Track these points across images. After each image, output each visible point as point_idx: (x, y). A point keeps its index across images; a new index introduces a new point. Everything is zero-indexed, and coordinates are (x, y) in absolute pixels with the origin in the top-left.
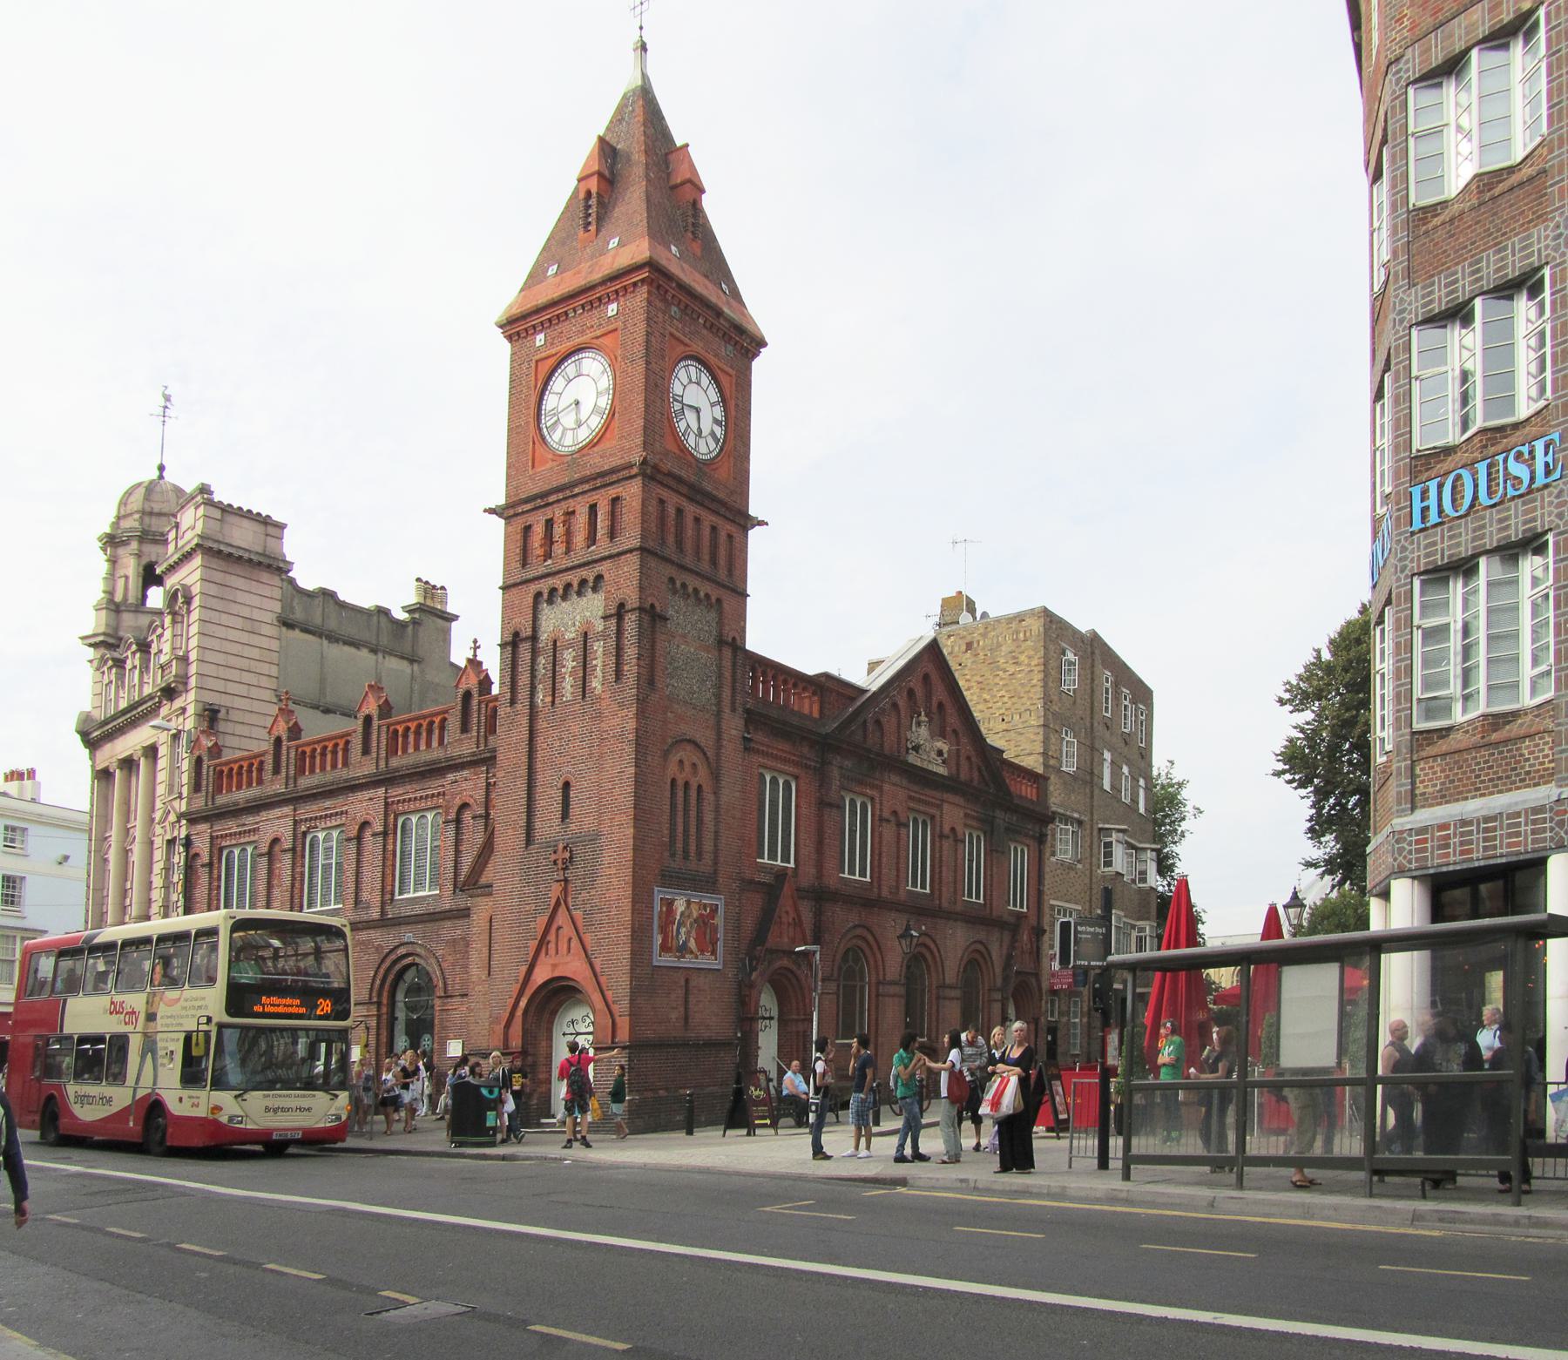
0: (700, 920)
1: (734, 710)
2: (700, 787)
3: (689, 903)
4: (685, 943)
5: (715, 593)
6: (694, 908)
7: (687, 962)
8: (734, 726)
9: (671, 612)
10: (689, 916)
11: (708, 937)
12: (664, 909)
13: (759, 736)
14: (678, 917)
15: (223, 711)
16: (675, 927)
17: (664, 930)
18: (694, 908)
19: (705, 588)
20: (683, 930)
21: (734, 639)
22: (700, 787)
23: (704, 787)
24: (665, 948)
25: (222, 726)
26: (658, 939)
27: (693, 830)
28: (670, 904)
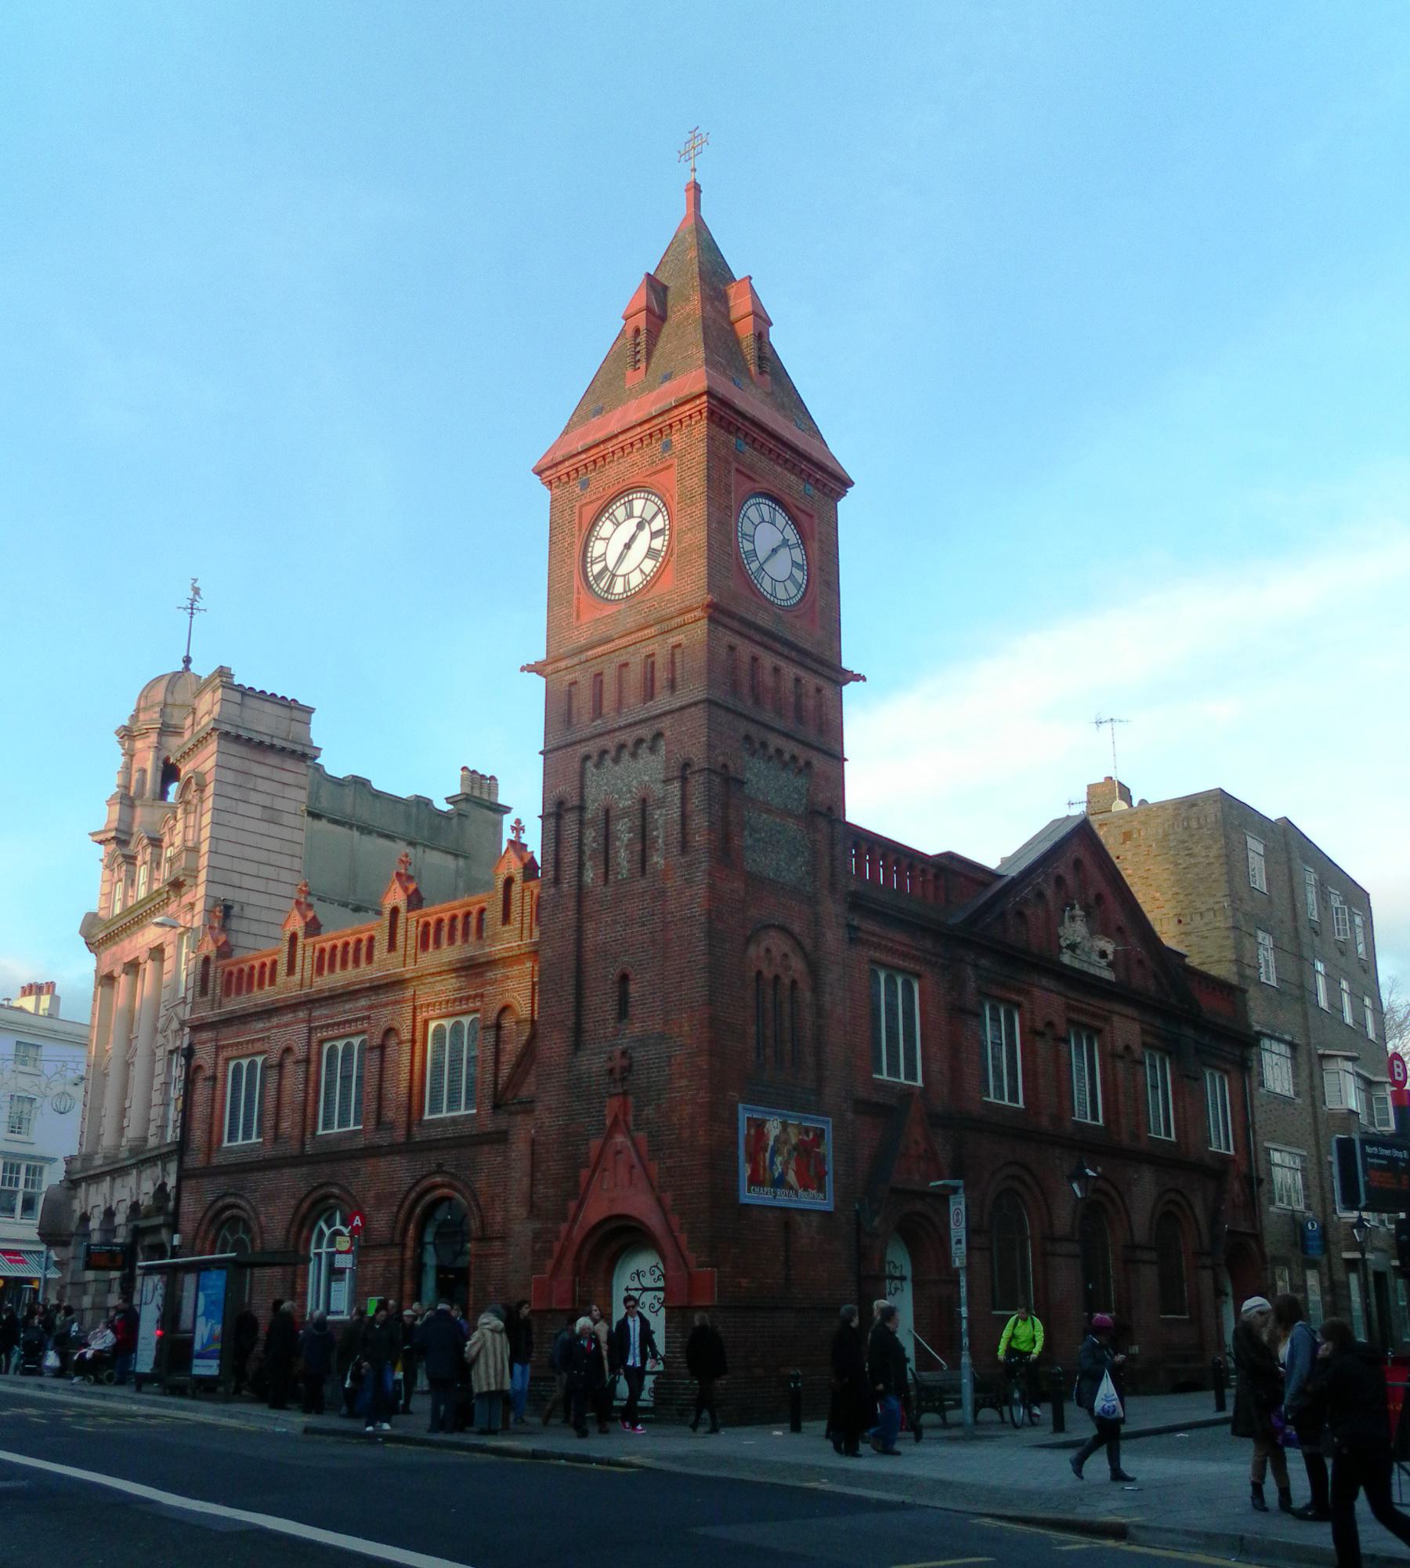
2: (794, 982)
3: (785, 1125)
4: (783, 1175)
5: (803, 754)
6: (792, 1132)
7: (784, 1199)
12: (753, 1132)
14: (771, 1143)
16: (768, 1155)
17: (753, 1158)
18: (792, 1132)
19: (790, 748)
20: (779, 1160)
22: (794, 982)
23: (801, 985)
24: (755, 1181)
28: (759, 1126)
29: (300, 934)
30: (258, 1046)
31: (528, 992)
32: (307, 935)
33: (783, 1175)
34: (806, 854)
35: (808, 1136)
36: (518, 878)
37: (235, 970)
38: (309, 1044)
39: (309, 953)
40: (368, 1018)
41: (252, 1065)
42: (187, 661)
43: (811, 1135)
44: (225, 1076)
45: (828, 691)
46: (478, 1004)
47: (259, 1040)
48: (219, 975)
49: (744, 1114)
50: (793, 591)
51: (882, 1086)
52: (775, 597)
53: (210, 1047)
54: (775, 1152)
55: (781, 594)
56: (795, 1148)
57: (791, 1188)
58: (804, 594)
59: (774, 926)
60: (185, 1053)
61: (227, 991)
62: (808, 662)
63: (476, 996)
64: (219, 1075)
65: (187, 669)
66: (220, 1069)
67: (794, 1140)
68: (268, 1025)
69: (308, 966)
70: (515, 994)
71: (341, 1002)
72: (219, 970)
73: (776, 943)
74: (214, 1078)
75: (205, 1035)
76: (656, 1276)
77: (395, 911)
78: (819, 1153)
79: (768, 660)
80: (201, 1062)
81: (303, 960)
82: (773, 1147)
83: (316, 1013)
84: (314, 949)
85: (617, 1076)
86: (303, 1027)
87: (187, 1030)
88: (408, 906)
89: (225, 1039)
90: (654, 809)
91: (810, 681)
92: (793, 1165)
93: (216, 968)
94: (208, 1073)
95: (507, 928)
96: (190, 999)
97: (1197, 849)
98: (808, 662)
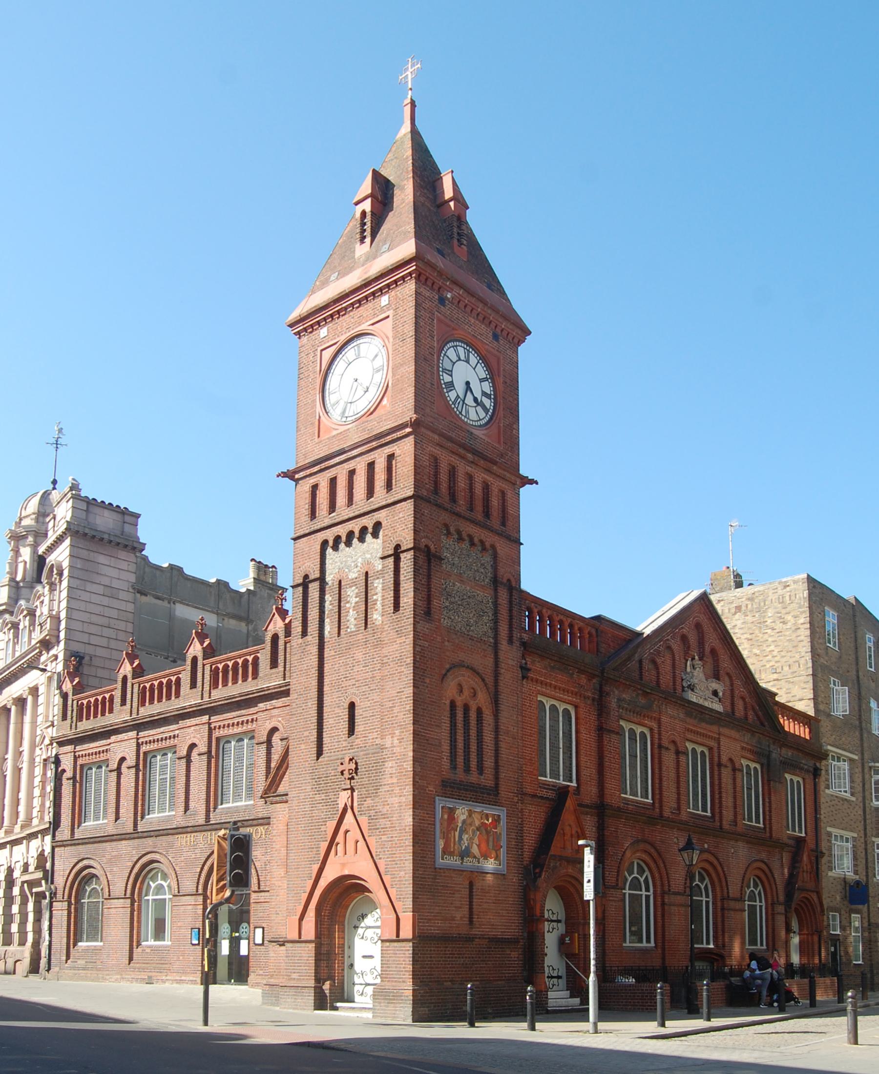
12: (446, 817)
16: (457, 834)
17: (446, 836)
24: (445, 851)
28: (451, 811)
50: (482, 414)
52: (468, 419)
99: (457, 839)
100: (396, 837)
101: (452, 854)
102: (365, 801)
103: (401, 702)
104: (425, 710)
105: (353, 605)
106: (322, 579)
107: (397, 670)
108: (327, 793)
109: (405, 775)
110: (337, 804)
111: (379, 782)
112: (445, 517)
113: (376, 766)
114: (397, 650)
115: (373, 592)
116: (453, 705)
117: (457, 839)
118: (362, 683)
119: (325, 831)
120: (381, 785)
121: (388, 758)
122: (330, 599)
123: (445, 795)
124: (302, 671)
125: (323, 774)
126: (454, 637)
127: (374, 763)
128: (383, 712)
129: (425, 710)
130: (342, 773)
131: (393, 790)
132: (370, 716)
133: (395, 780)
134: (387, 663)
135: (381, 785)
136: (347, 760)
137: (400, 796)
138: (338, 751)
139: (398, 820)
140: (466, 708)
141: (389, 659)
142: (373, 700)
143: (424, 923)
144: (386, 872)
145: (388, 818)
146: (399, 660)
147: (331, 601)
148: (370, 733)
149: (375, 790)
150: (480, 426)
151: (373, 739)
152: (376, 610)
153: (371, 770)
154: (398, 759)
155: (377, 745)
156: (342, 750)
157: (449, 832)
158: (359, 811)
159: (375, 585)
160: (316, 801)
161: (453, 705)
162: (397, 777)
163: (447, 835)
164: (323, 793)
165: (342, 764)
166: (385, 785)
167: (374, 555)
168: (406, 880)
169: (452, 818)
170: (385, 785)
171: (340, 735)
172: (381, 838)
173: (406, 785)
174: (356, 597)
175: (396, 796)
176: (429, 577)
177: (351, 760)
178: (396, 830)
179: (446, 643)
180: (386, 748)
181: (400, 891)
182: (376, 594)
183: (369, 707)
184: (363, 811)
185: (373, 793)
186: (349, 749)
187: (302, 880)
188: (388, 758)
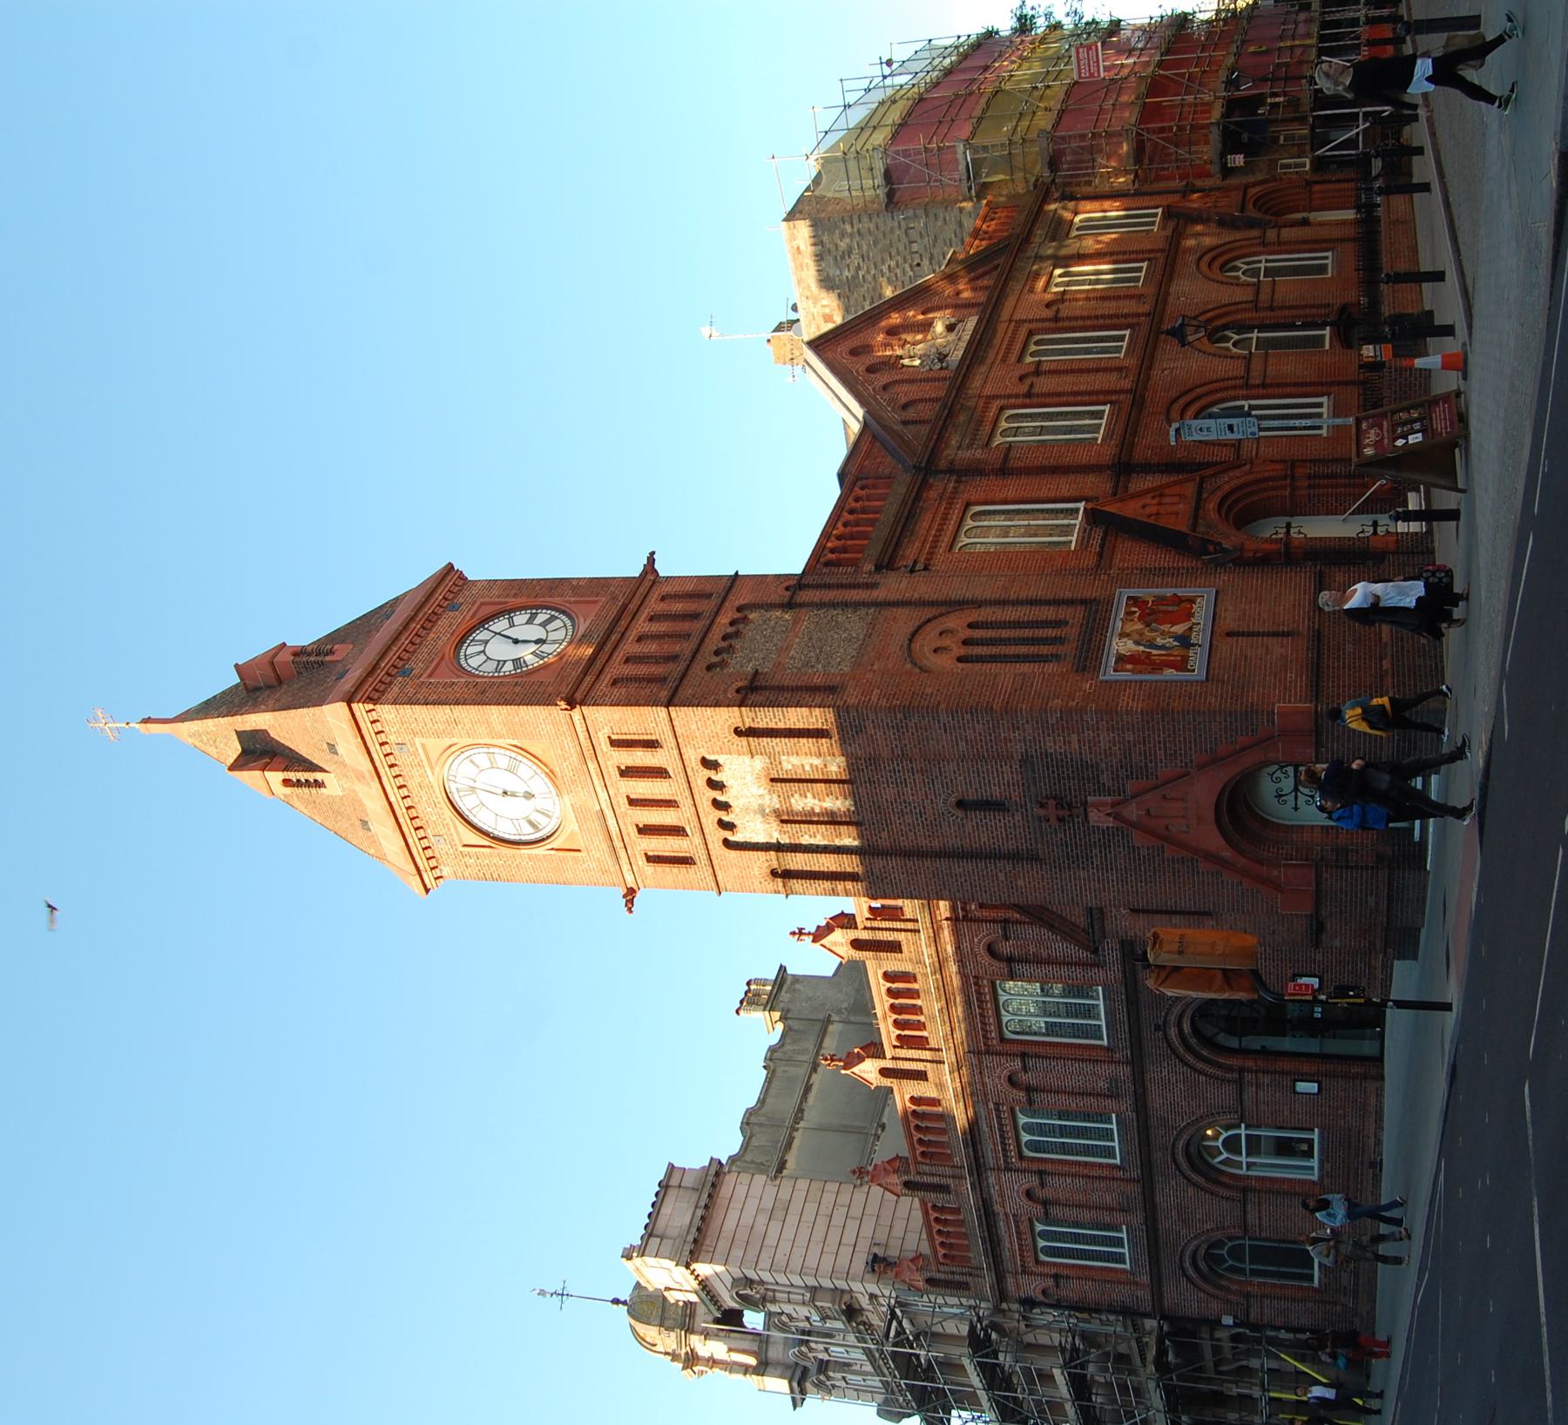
0: (1147, 619)
1: (874, 586)
2: (970, 626)
3: (1122, 635)
4: (1177, 638)
6: (1130, 628)
7: (1200, 636)
8: (894, 585)
9: (749, 669)
10: (1141, 634)
11: (1170, 608)
12: (1129, 666)
13: (910, 552)
14: (1141, 648)
15: (876, 1250)
16: (1154, 652)
17: (1157, 667)
18: (1130, 628)
20: (1159, 641)
21: (787, 589)
22: (970, 626)
23: (970, 620)
24: (1182, 665)
25: (893, 1253)
26: (1170, 674)
27: (1027, 633)
28: (1121, 659)
29: (906, 1178)
30: (1024, 1227)
31: (974, 926)
32: (907, 1172)
33: (1177, 638)
34: (836, 612)
35: (1135, 612)
36: (853, 934)
37: (942, 1252)
38: (1024, 1171)
39: (927, 1169)
40: (997, 1104)
41: (1045, 1235)
42: (616, 1301)
43: (1133, 609)
44: (1055, 1264)
45: (666, 589)
46: (985, 981)
47: (1017, 1227)
48: (947, 1269)
49: (1110, 674)
50: (557, 623)
51: (1083, 542)
52: (563, 641)
53: (1023, 1280)
54: (1152, 645)
55: (560, 635)
56: (1148, 625)
57: (1190, 629)
58: (563, 612)
59: (909, 645)
60: (1027, 1308)
61: (964, 1260)
62: (632, 607)
63: (976, 984)
64: (1053, 1271)
65: (625, 1303)
66: (1047, 1270)
67: (1139, 626)
68: (1002, 1216)
69: (940, 1170)
70: (976, 940)
71: (979, 1135)
72: (941, 1268)
73: (929, 639)
74: (1056, 1277)
75: (1010, 1283)
76: (1282, 776)
77: (884, 1072)
78: (1153, 601)
79: (629, 647)
80: (1038, 1290)
81: (933, 1175)
82: (1145, 646)
83: (991, 1162)
84: (922, 1163)
85: (1066, 813)
86: (1005, 1177)
87: (1004, 1306)
88: (879, 1058)
89: (1016, 1264)
90: (782, 769)
91: (653, 605)
92: (1166, 627)
93: (939, 1271)
94: (1050, 1282)
95: (904, 948)
96: (972, 1302)
97: (843, 245)
98: (632, 607)
99: (1164, 652)
100: (1159, 736)
101: (1185, 659)
102: (1104, 784)
103: (960, 728)
104: (971, 694)
105: (816, 802)
106: (778, 848)
107: (913, 734)
108: (1090, 845)
109: (1067, 723)
110: (1108, 828)
111: (1077, 762)
112: (698, 669)
113: (1053, 766)
114: (885, 733)
115: (800, 771)
116: (960, 659)
117: (1164, 652)
118: (930, 789)
119: (1148, 849)
120: (1081, 759)
121: (1040, 748)
122: (807, 837)
123: (1097, 669)
124: (909, 881)
125: (1063, 851)
126: (866, 657)
127: (1048, 769)
128: (974, 755)
129: (971, 694)
130: (1060, 820)
131: (1089, 741)
132: (979, 776)
133: (1074, 738)
134: (902, 748)
135: (1081, 759)
136: (1042, 812)
137: (1098, 728)
138: (1029, 827)
139: (1134, 733)
140: (966, 642)
141: (896, 746)
142: (955, 772)
143: (1290, 696)
144: (1211, 752)
145: (1130, 749)
146: (898, 731)
147: (810, 836)
148: (1003, 778)
149: (1087, 769)
150: (573, 625)
151: (1012, 772)
152: (825, 766)
153: (1058, 775)
154: (1043, 732)
155: (1021, 767)
156: (1028, 821)
157: (1153, 663)
158: (1120, 795)
159: (790, 767)
160: (1102, 863)
161: (960, 659)
162: (1069, 735)
163: (1158, 664)
164: (1091, 852)
165: (1048, 820)
166: (1081, 754)
167: (749, 769)
168: (1226, 721)
169: (1132, 659)
170: (1081, 754)
171: (1005, 824)
172: (1161, 760)
173: (1082, 720)
174: (806, 797)
175: (1099, 736)
176: (781, 689)
177: (1042, 806)
178: (1149, 735)
179: (875, 667)
180: (1026, 750)
181: (1241, 730)
182: (803, 765)
183: (965, 778)
184: (1119, 788)
185: (1093, 772)
186: (1026, 810)
187: (1223, 888)
188: (1040, 748)
